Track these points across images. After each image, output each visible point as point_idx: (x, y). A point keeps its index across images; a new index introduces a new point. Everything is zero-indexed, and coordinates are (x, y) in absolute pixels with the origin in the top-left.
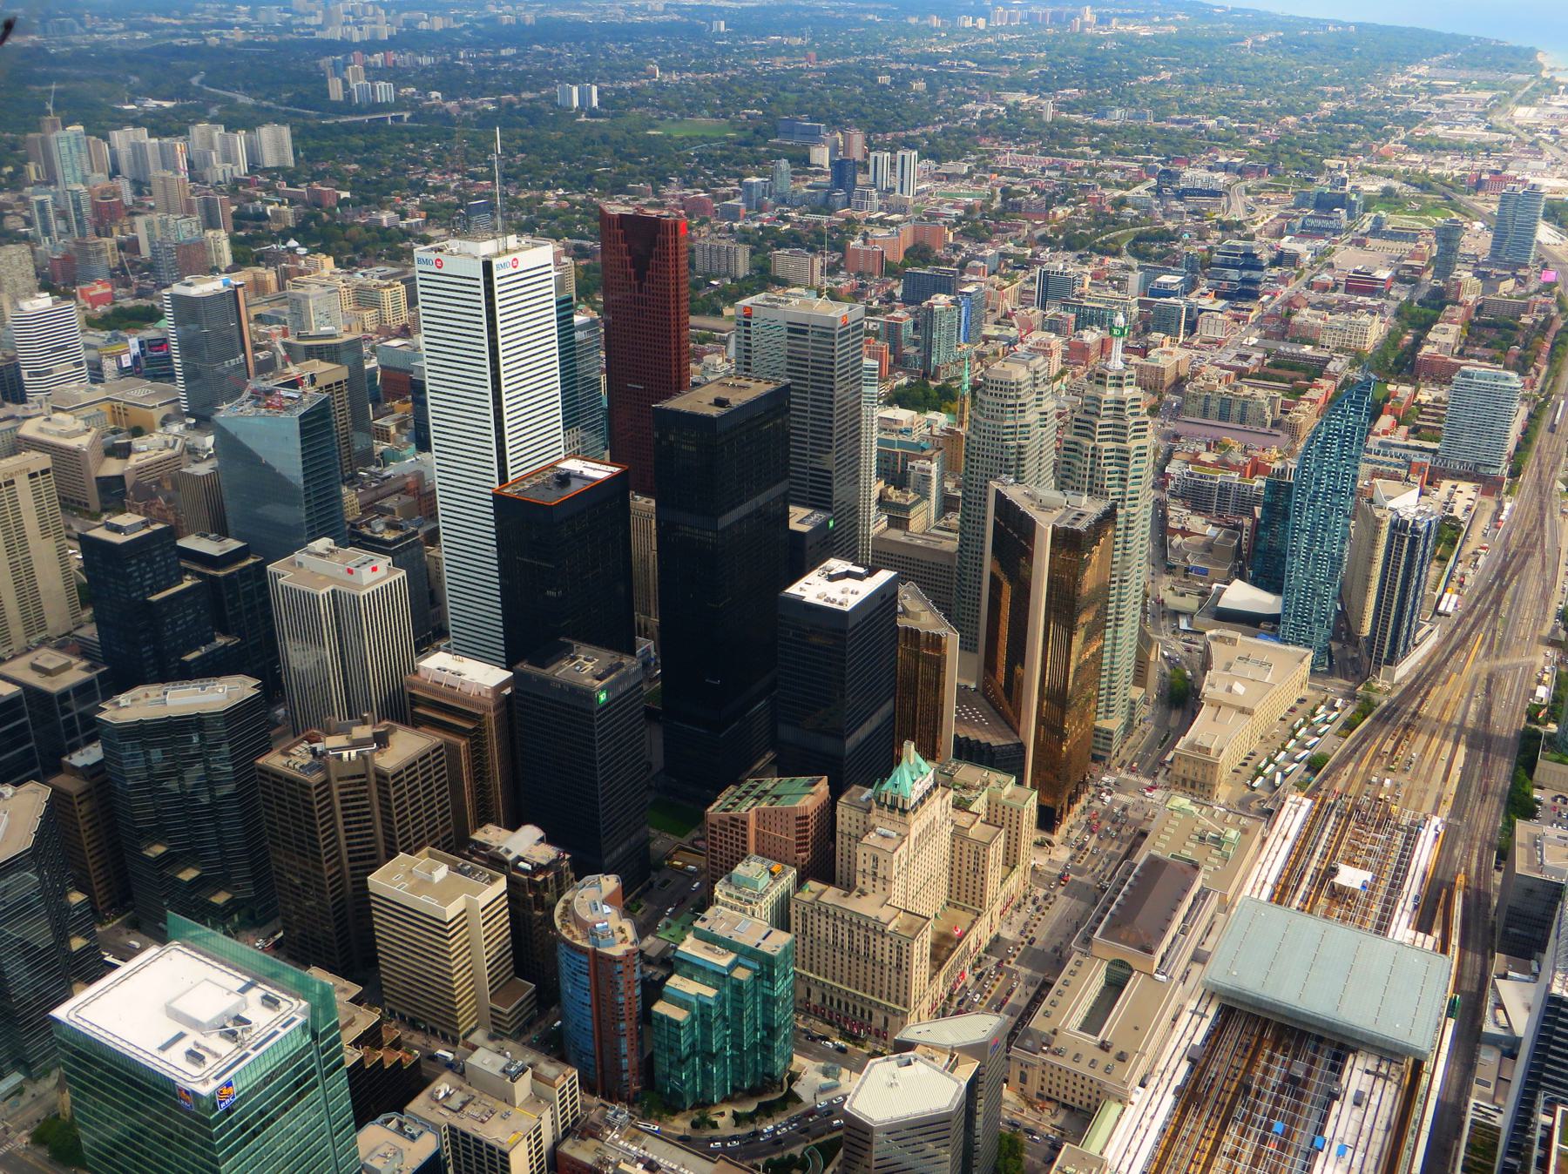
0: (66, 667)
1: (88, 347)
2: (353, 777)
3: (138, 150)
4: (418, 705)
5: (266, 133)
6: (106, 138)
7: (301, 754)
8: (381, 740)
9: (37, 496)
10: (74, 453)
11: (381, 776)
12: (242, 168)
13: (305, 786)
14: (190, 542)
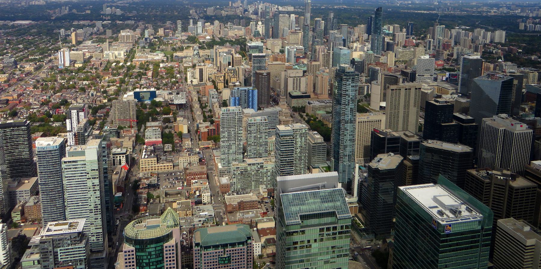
0: (413, 136)
1: (435, 74)
2: (500, 185)
3: (458, 34)
4: (528, 175)
5: (497, 33)
6: (450, 30)
7: (483, 173)
8: (514, 178)
9: (416, 95)
10: (426, 94)
11: (511, 188)
12: (488, 41)
13: (483, 182)
14: (457, 114)
